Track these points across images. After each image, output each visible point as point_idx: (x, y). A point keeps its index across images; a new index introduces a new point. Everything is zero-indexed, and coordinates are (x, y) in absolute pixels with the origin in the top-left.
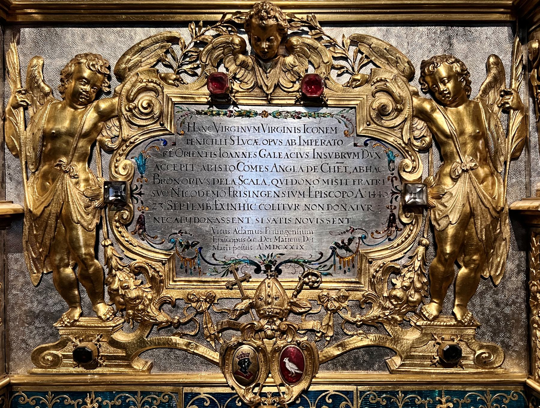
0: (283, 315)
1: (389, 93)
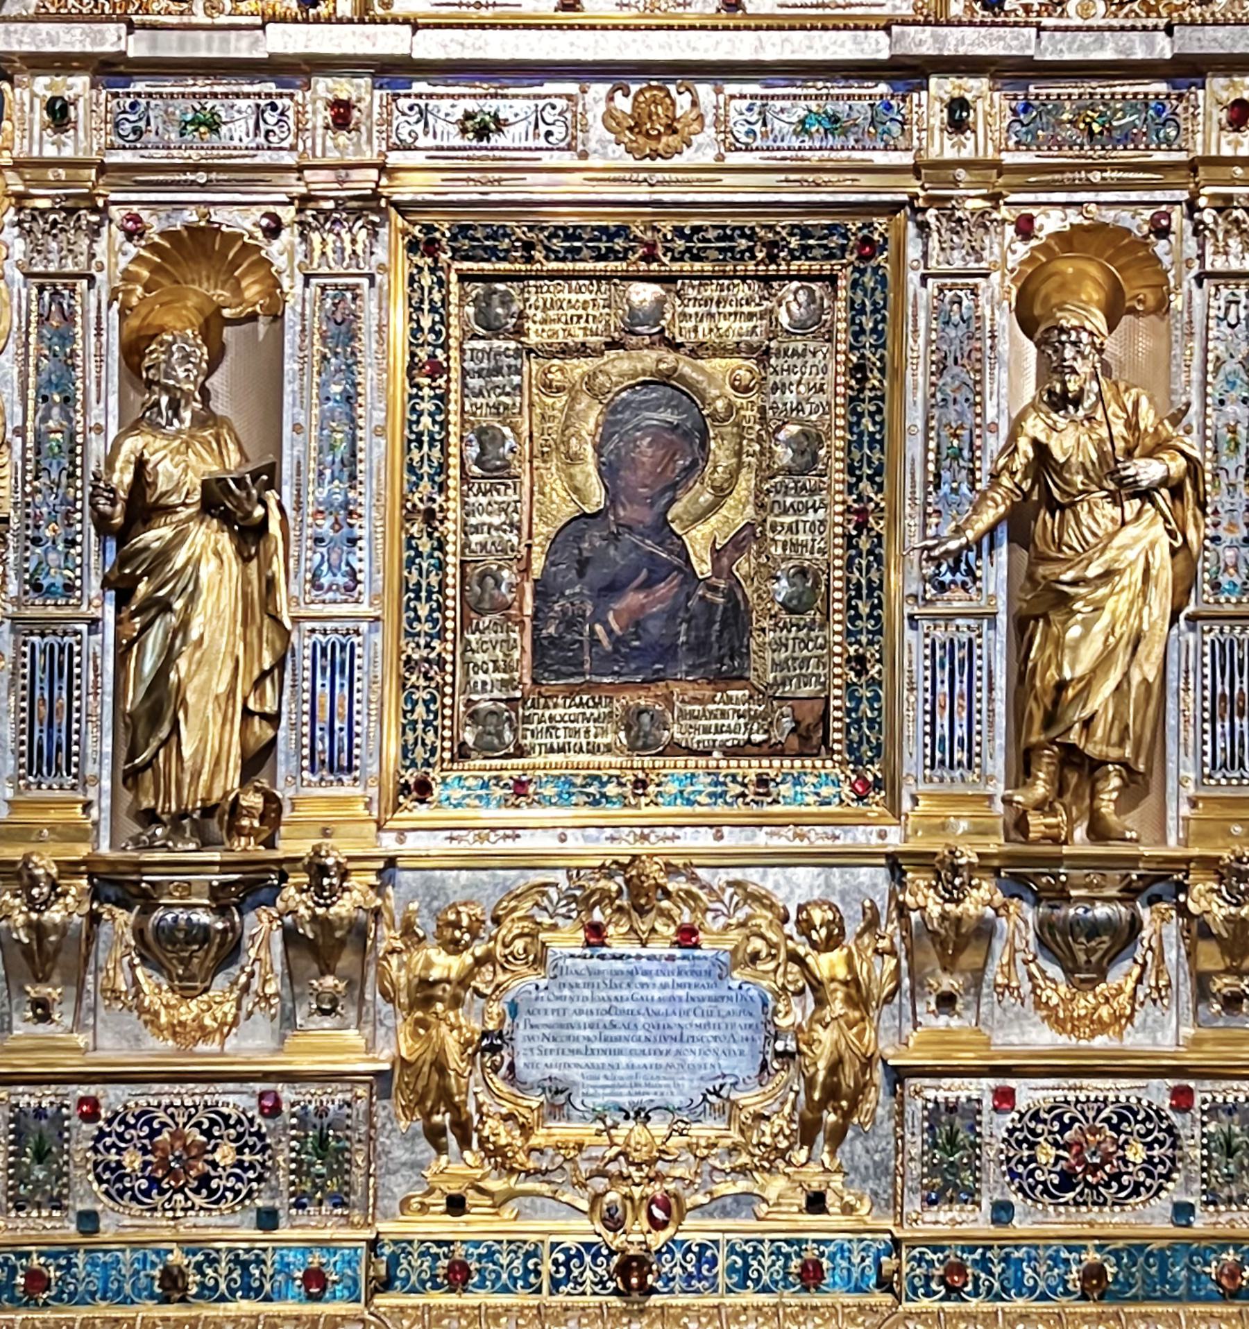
0: (651, 1162)
1: (762, 937)
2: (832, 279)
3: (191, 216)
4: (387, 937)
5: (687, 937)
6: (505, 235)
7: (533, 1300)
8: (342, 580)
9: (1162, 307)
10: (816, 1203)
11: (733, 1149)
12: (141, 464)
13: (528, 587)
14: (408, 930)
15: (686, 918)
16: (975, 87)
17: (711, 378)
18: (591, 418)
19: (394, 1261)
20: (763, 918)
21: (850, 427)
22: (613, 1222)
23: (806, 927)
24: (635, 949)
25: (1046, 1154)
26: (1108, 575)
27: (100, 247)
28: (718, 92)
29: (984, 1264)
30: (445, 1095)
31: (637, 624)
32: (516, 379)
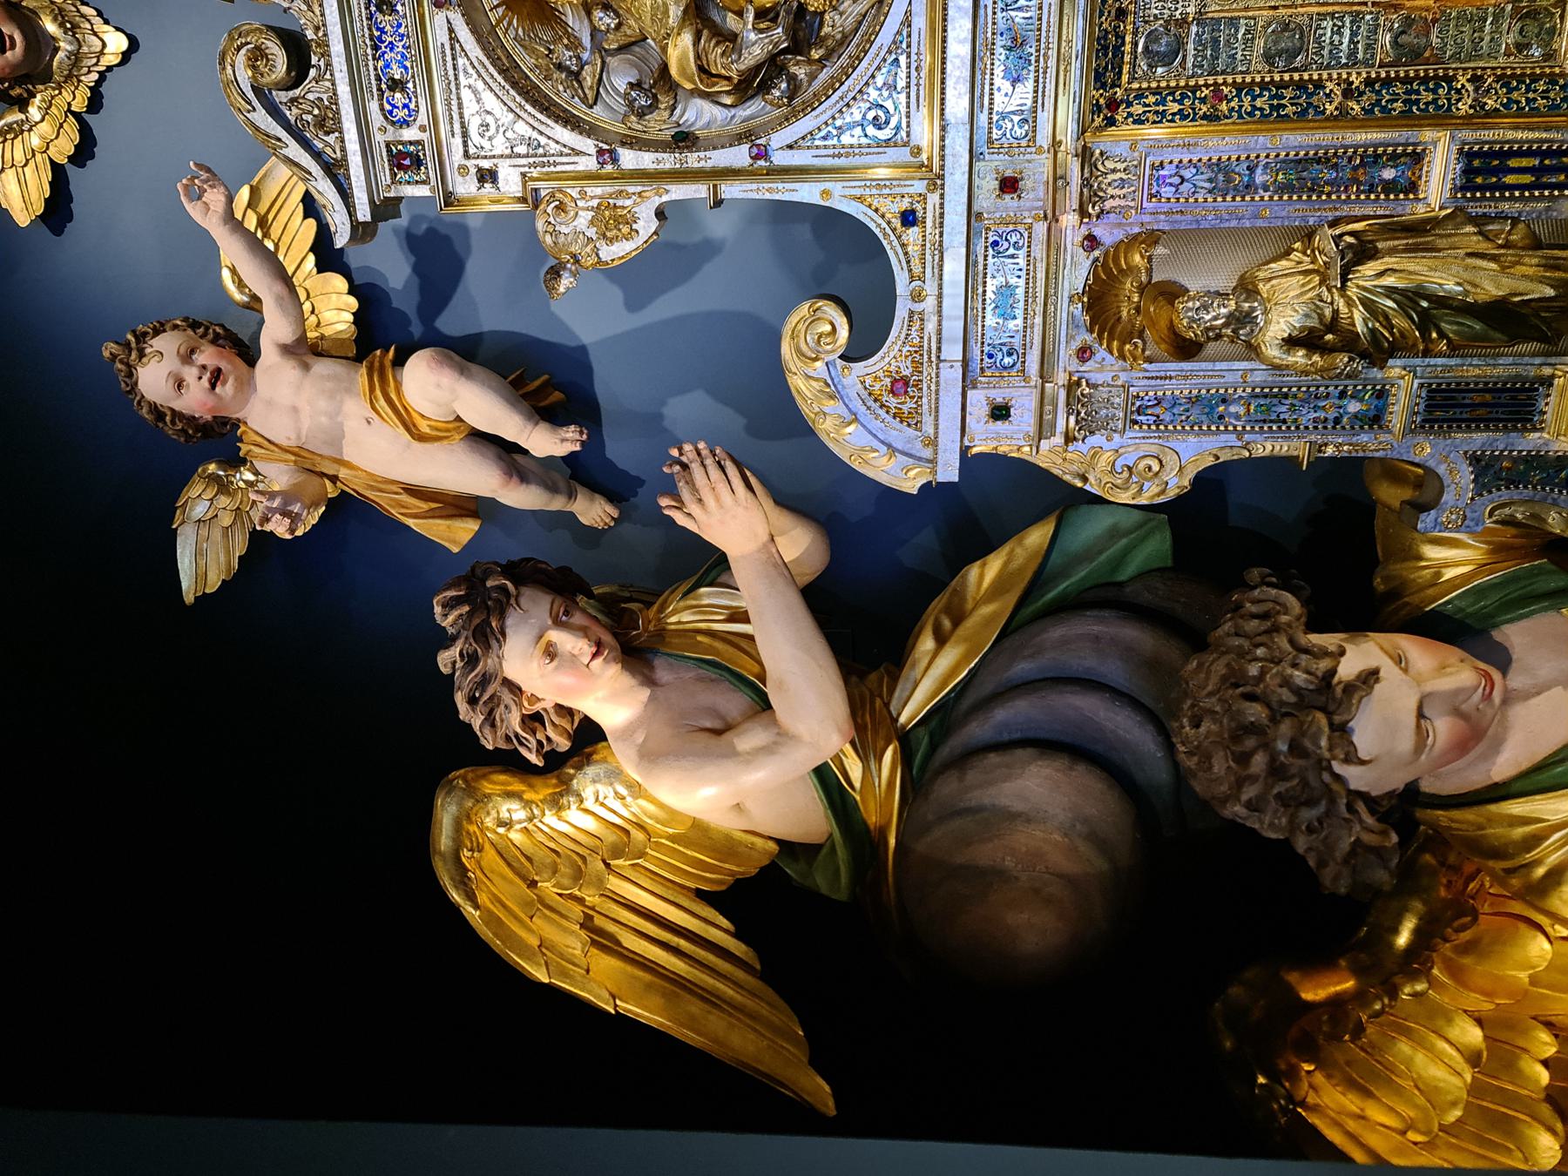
6: (1105, 38)
27: (1097, 378)
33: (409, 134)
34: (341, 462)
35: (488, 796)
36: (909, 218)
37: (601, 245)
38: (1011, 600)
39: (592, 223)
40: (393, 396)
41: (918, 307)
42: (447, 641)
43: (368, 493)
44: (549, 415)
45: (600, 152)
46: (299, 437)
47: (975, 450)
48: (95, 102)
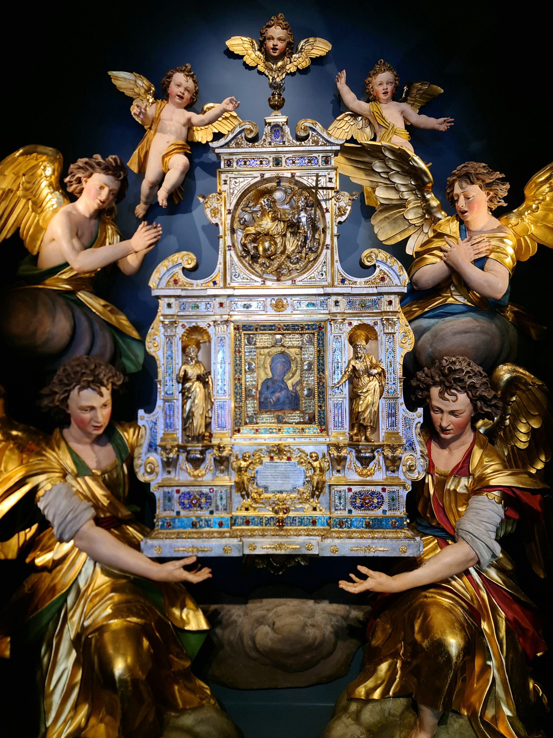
0: (283, 501)
2: (314, 334)
3: (194, 324)
4: (233, 459)
5: (289, 459)
7: (262, 527)
8: (223, 392)
9: (376, 339)
10: (315, 509)
11: (299, 499)
12: (185, 371)
13: (258, 392)
14: (237, 457)
15: (289, 455)
16: (339, 298)
17: (291, 353)
18: (269, 360)
19: (235, 520)
20: (303, 455)
21: (318, 362)
22: (276, 512)
23: (311, 457)
24: (279, 461)
25: (358, 501)
26: (367, 391)
27: (177, 330)
28: (291, 299)
29: (347, 522)
30: (244, 489)
31: (278, 399)
32: (255, 353)
33: (235, 164)
34: (156, 132)
35: (54, 164)
36: (215, 283)
37: (210, 209)
38: (117, 325)
39: (215, 207)
40: (176, 151)
41: (195, 285)
42: (104, 158)
43: (145, 140)
44: (171, 196)
45: (230, 210)
46: (163, 120)
47: (160, 301)
48: (260, 73)
